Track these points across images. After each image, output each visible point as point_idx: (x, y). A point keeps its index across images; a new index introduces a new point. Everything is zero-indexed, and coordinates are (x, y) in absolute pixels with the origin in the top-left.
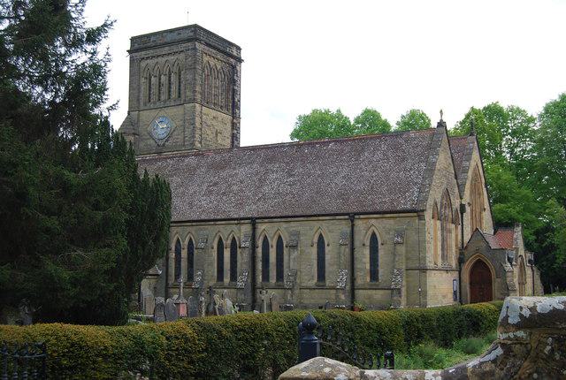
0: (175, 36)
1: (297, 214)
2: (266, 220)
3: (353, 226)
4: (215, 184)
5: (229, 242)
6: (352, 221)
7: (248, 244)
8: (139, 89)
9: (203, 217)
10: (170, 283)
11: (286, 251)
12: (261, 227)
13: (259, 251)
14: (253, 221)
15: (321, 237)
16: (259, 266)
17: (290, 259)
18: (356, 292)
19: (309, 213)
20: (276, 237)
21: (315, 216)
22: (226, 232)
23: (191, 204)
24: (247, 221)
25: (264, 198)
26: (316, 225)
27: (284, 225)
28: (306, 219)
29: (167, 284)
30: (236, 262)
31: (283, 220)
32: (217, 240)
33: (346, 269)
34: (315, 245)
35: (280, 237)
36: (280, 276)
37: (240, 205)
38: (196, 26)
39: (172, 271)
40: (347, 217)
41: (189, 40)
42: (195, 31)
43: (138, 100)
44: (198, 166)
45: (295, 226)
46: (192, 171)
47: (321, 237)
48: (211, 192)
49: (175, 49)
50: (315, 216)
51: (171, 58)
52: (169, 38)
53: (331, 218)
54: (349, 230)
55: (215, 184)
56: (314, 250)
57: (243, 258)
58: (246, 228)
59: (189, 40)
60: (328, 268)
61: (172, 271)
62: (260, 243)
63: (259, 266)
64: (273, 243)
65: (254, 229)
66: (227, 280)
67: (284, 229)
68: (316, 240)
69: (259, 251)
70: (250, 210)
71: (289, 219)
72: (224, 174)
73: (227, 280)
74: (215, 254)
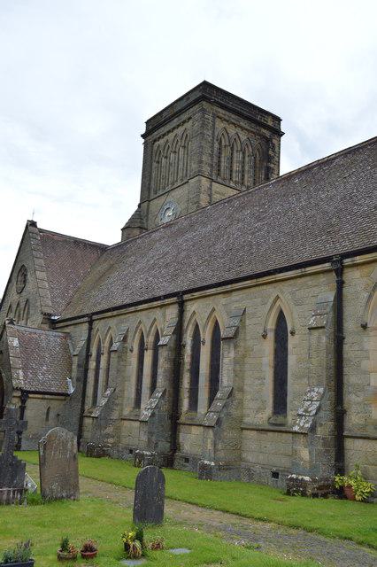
0: (184, 103)
1: (242, 275)
2: (197, 294)
3: (340, 285)
6: (339, 272)
10: (86, 407)
12: (191, 308)
13: (188, 350)
14: (180, 299)
15: (281, 318)
18: (349, 443)
19: (261, 269)
26: (272, 291)
27: (222, 300)
29: (83, 410)
31: (220, 289)
33: (318, 385)
34: (271, 336)
35: (217, 324)
40: (327, 266)
41: (196, 102)
45: (238, 301)
47: (281, 318)
49: (184, 117)
51: (180, 131)
52: (178, 108)
53: (298, 272)
54: (331, 296)
56: (269, 346)
58: (172, 312)
59: (196, 102)
60: (292, 386)
62: (188, 339)
64: (206, 336)
68: (271, 325)
69: (188, 350)
71: (229, 287)
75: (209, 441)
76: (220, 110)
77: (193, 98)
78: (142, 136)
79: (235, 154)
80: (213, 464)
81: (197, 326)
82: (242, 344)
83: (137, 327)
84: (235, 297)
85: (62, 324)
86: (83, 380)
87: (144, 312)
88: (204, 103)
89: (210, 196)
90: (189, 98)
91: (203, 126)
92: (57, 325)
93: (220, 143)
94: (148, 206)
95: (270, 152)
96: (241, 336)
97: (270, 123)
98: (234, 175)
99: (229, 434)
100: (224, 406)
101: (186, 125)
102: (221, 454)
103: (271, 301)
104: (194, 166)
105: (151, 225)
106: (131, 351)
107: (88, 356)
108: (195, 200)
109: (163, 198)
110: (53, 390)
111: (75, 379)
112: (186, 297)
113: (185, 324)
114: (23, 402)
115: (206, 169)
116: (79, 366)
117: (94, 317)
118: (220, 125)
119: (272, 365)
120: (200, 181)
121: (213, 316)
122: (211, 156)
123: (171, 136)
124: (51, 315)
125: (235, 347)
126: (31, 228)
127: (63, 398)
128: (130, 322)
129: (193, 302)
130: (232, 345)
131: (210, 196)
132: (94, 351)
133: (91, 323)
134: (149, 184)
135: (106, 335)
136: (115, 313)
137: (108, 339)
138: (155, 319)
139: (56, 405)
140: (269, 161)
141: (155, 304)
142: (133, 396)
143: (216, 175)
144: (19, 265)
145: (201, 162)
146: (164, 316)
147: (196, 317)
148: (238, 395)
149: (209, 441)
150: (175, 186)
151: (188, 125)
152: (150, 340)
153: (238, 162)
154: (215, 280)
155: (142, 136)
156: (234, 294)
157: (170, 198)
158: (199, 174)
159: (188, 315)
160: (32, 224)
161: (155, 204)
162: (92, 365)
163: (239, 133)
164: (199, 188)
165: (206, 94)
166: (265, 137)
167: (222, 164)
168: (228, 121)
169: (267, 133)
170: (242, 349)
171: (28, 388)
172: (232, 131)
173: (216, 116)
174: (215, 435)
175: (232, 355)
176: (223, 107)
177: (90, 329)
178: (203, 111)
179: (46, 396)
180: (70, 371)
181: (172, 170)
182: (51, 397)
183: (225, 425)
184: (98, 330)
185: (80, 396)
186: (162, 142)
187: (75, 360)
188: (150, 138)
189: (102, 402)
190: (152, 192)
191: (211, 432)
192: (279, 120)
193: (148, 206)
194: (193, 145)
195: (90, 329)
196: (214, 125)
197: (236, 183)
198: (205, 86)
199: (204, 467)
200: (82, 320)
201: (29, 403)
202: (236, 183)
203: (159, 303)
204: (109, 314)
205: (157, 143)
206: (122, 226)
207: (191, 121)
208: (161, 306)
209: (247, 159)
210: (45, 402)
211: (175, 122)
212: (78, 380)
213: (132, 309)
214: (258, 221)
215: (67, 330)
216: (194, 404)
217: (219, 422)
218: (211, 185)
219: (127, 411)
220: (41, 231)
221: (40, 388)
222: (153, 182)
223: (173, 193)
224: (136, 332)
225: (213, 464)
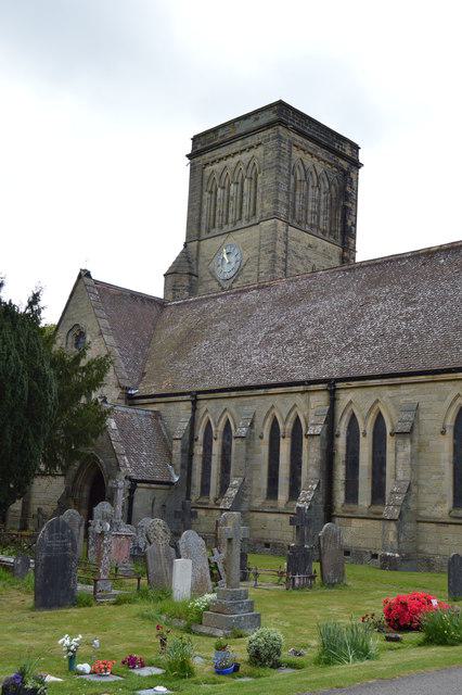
1: (413, 369)
2: (354, 384)
4: (279, 328)
5: (289, 426)
7: (318, 429)
8: (200, 209)
9: (249, 382)
10: (193, 498)
11: (390, 443)
12: (345, 397)
13: (341, 443)
14: (332, 386)
16: (340, 472)
17: (397, 458)
19: (436, 365)
20: (372, 417)
21: (449, 371)
22: (283, 406)
23: (235, 363)
24: (320, 386)
25: (357, 346)
27: (388, 392)
28: (430, 378)
30: (300, 464)
31: (385, 381)
32: (269, 422)
34: (450, 432)
35: (380, 416)
36: (378, 493)
37: (313, 359)
38: (281, 104)
39: (197, 478)
41: (269, 125)
42: (279, 112)
43: (199, 225)
44: (259, 304)
45: (408, 394)
46: (248, 311)
48: (268, 341)
49: (251, 141)
50: (449, 371)
51: (245, 156)
52: (243, 127)
55: (279, 328)
57: (311, 454)
58: (319, 401)
59: (269, 125)
61: (197, 478)
62: (342, 428)
63: (340, 472)
64: (366, 427)
65: (333, 401)
66: (283, 496)
67: (391, 402)
69: (341, 443)
70: (330, 367)
71: (398, 380)
72: (295, 312)
73: (283, 496)
74: (264, 448)
75: (391, 533)
76: (297, 137)
77: (264, 120)
78: (188, 156)
79: (311, 190)
80: (397, 555)
81: (353, 416)
82: (416, 439)
83: (268, 412)
84: (404, 390)
85: (145, 401)
86: (187, 467)
87: (278, 396)
88: (281, 128)
89: (286, 243)
90: (257, 119)
91: (279, 157)
92: (137, 401)
93: (296, 178)
94: (198, 247)
95: (348, 189)
96: (416, 430)
97: (348, 153)
98: (309, 216)
99: (409, 527)
100: (405, 500)
101: (253, 152)
102: (403, 546)
103: (450, 398)
104: (268, 206)
105: (203, 271)
106: (261, 437)
107: (192, 439)
108: (270, 248)
109: (221, 240)
110: (158, 478)
111: (178, 466)
112: (339, 385)
113: (339, 414)
114: (132, 491)
115: (283, 211)
116: (183, 451)
117: (200, 396)
118: (297, 154)
119: (452, 459)
120: (276, 225)
121: (376, 408)
122: (287, 194)
123: (232, 162)
124: (128, 389)
125: (411, 441)
126: (86, 280)
127: (168, 487)
128: (259, 406)
129: (348, 391)
130: (408, 441)
131: (286, 243)
132: (200, 434)
133: (195, 402)
134: (200, 219)
135: (221, 417)
136: (233, 394)
137: (222, 422)
138: (295, 405)
139: (161, 493)
140: (347, 200)
141: (295, 389)
142: (264, 486)
143: (294, 219)
144: (70, 324)
145: (276, 202)
146: (308, 403)
147: (353, 407)
148: (414, 489)
149: (391, 533)
150: (239, 225)
151: (259, 151)
152: (286, 427)
153: (314, 200)
154: (378, 371)
155: (188, 156)
156: (402, 387)
157: (231, 239)
158: (276, 216)
159: (341, 405)
160: (84, 275)
161: (208, 246)
162: (199, 450)
163: (312, 161)
164: (275, 233)
165: (282, 117)
166: (343, 170)
167: (297, 203)
168: (318, 158)
169: (345, 164)
170: (416, 444)
171: (134, 476)
172: (309, 161)
173: (291, 144)
174: (398, 527)
175: (408, 449)
176: (300, 133)
177: (194, 409)
178: (279, 137)
179: (153, 486)
180: (170, 455)
181: (232, 205)
182: (158, 486)
183: (405, 518)
184: (207, 411)
185: (184, 485)
186: (216, 167)
187: (178, 444)
188: (200, 160)
189: (232, 493)
190: (203, 230)
191: (393, 526)
192: (355, 148)
193: (198, 247)
194: (266, 180)
195: (194, 409)
196: (290, 156)
197: (312, 226)
198: (281, 107)
199: (386, 559)
200: (185, 398)
201: (138, 491)
202: (312, 226)
203: (301, 388)
204: (226, 394)
205: (209, 168)
206: (165, 270)
207: (261, 149)
208: (303, 392)
209: (323, 196)
210: (150, 491)
211: (238, 145)
212: (182, 467)
213: (262, 391)
214: (409, 304)
215: (155, 408)
216: (352, 495)
217: (401, 515)
218: (287, 230)
219: (258, 502)
220: (96, 282)
221: (146, 477)
222: (204, 217)
223: (237, 235)
224: (266, 418)
225: (397, 555)
